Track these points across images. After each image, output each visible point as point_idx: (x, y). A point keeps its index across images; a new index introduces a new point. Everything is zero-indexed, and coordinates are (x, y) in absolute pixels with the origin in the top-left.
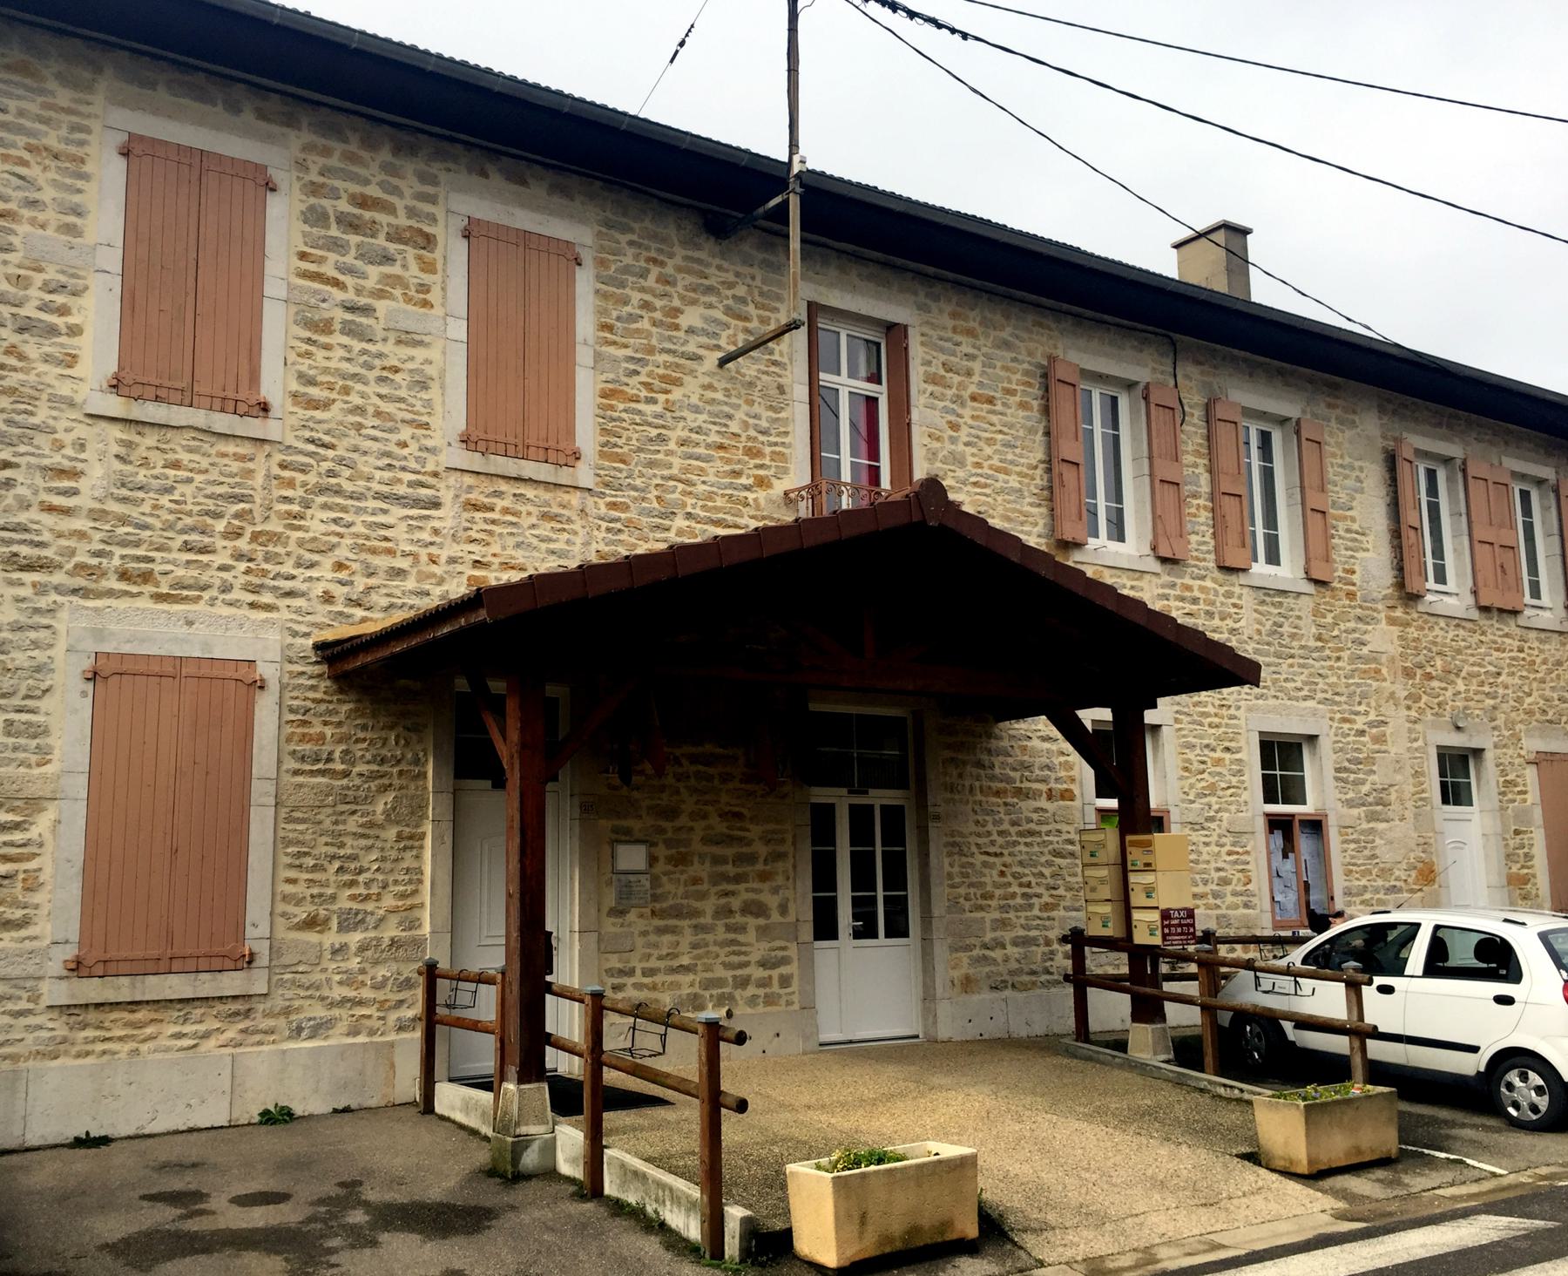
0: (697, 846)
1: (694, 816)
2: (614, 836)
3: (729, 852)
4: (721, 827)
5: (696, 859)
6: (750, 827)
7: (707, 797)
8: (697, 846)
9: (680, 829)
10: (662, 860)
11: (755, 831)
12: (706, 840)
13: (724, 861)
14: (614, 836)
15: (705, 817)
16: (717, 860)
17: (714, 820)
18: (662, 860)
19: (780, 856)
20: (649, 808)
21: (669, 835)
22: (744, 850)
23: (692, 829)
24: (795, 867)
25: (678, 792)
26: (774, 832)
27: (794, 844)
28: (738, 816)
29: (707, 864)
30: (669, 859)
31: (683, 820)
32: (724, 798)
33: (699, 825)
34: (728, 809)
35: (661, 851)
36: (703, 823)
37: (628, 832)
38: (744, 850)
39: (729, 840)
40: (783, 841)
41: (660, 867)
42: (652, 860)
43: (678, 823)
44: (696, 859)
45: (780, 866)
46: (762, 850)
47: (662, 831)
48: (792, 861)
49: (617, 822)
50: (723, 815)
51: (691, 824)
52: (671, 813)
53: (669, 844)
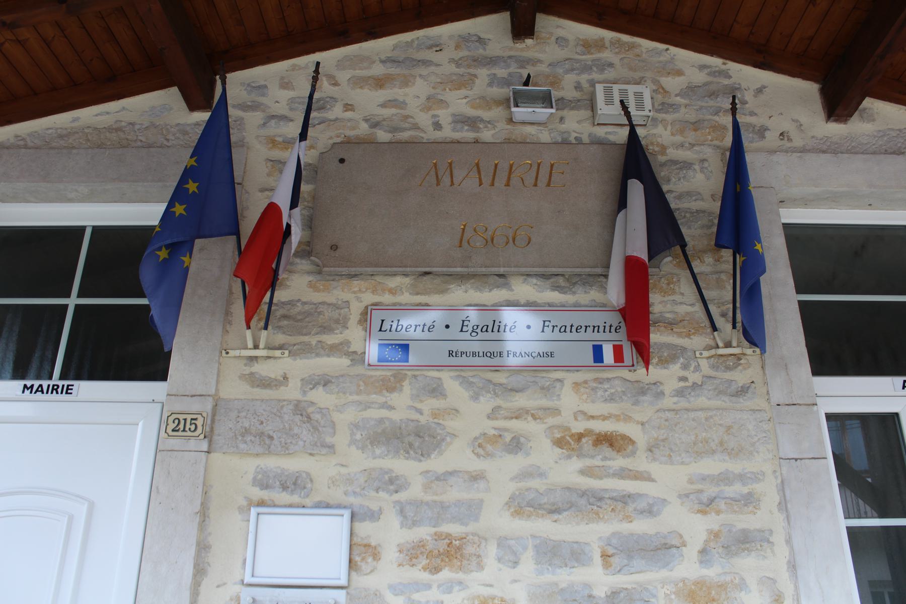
0: (497, 519)
1: (484, 445)
2: (257, 493)
3: (594, 533)
4: (567, 472)
5: (492, 551)
6: (655, 468)
7: (521, 401)
8: (497, 519)
9: (444, 477)
10: (390, 554)
11: (667, 478)
12: (521, 506)
13: (576, 555)
14: (257, 493)
15: (516, 445)
16: (552, 553)
17: (543, 453)
18: (390, 554)
19: (745, 542)
20: (355, 426)
21: (415, 491)
22: (641, 526)
23: (476, 477)
24: (793, 567)
25: (436, 390)
26: (725, 478)
27: (783, 506)
28: (611, 442)
29: (528, 566)
30: (413, 553)
31: (456, 456)
32: (569, 400)
33: (503, 469)
34: (579, 427)
35: (390, 533)
36: (515, 463)
37: (294, 484)
38: (641, 526)
39: (591, 503)
40: (749, 501)
41: (386, 574)
42: (360, 553)
43: (437, 463)
44: (492, 551)
45: (748, 565)
46: (696, 528)
47: (394, 483)
48: (782, 551)
49: (273, 463)
50: (569, 442)
51: (476, 465)
52: (418, 439)
53: (408, 514)
